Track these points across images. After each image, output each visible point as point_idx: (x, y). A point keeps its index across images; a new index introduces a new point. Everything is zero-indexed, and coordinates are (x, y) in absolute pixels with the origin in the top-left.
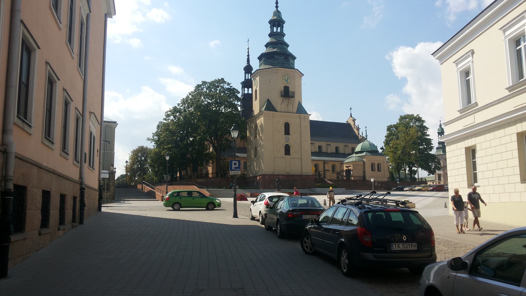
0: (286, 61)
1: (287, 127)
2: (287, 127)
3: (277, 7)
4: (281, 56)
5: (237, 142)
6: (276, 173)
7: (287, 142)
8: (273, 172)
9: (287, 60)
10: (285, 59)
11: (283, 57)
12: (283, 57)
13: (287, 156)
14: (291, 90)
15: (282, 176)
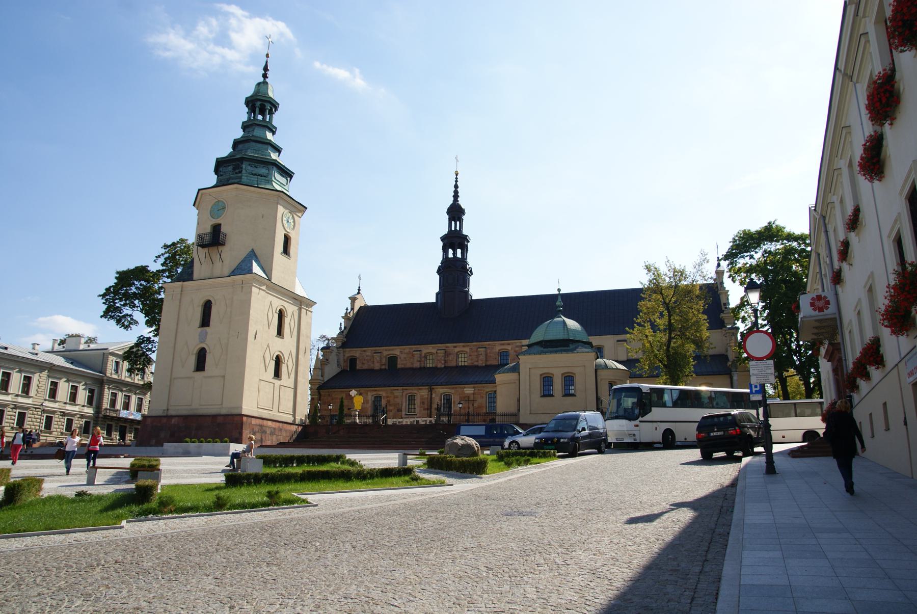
0: (236, 173)
1: (207, 307)
2: (207, 307)
3: (265, 76)
4: (229, 166)
5: (400, 358)
6: (171, 413)
7: (202, 342)
8: (164, 410)
9: (237, 171)
10: (234, 169)
11: (230, 168)
12: (230, 168)
13: (200, 374)
14: (223, 230)
15: (177, 418)
